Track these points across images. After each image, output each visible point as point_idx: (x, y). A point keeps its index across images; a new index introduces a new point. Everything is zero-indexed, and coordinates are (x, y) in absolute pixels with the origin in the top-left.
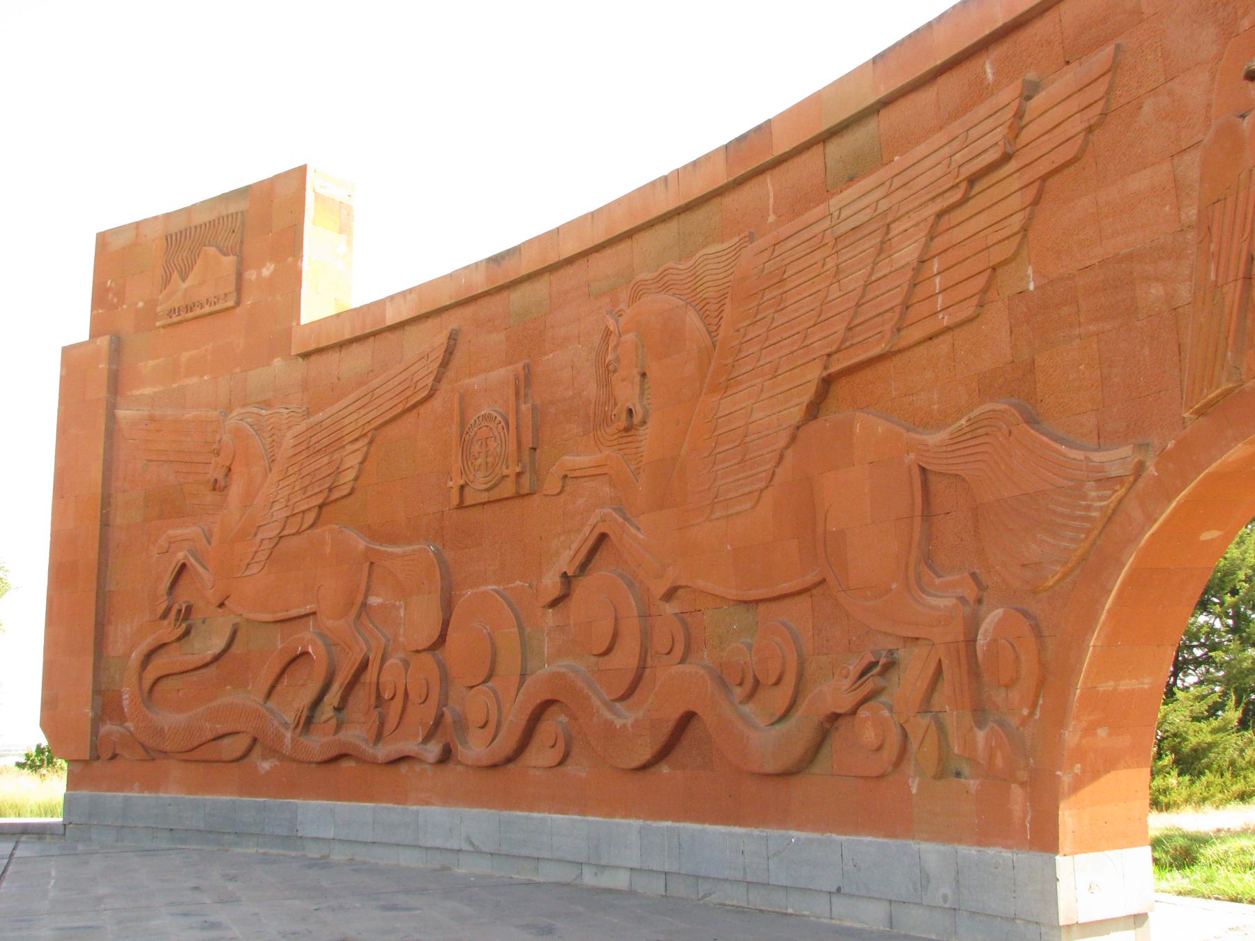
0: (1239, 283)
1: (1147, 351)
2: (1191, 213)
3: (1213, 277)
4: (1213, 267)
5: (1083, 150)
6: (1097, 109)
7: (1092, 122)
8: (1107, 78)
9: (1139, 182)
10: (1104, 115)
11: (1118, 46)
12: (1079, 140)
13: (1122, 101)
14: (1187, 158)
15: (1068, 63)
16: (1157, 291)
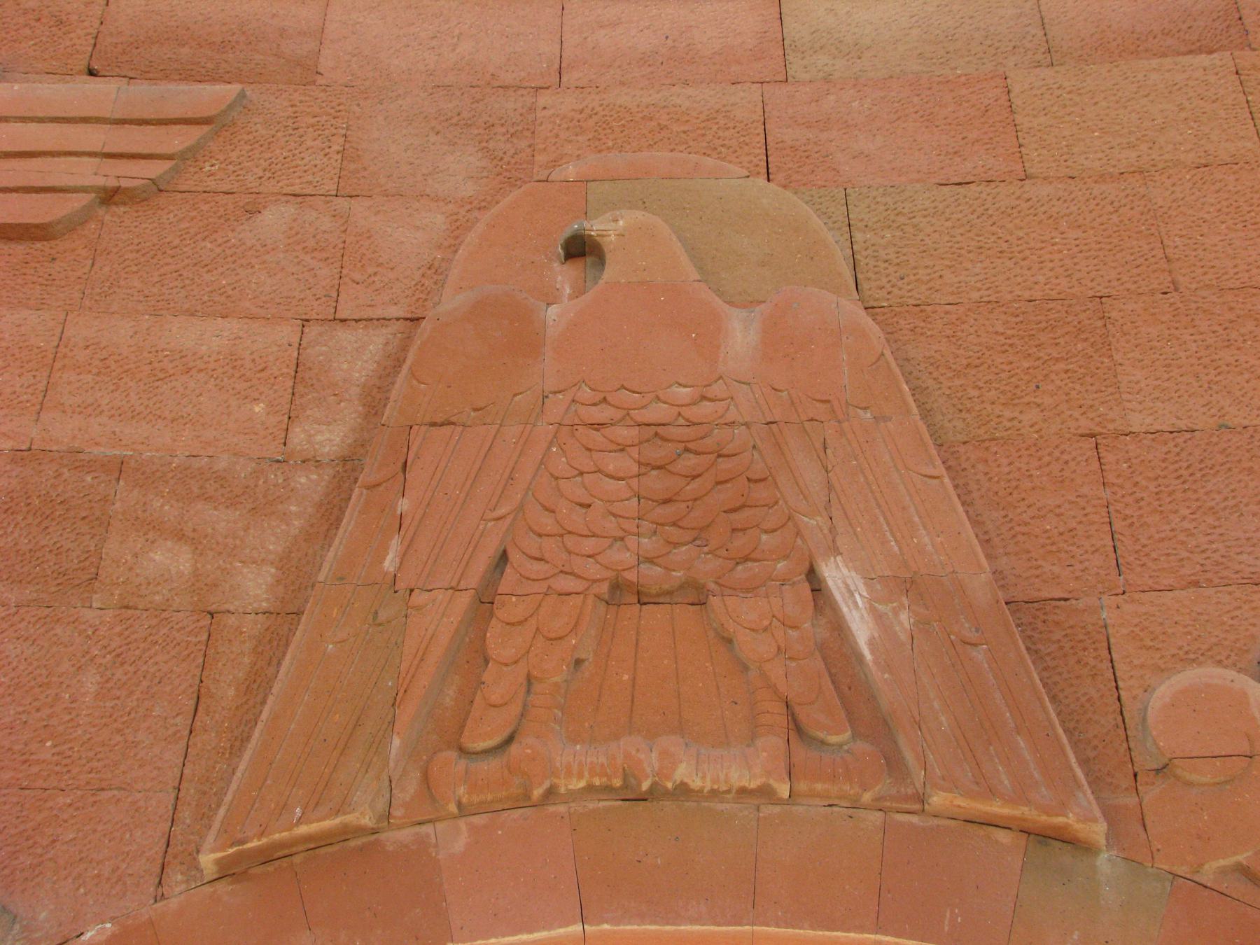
0: (464, 600)
1: (90, 682)
2: (327, 435)
3: (389, 564)
4: (395, 545)
5: (72, 225)
6: (155, 169)
7: (125, 183)
8: (196, 132)
9: (206, 337)
10: (158, 187)
11: (242, 95)
12: (77, 202)
13: (211, 184)
14: (345, 336)
15: (92, 73)
16: (169, 560)
